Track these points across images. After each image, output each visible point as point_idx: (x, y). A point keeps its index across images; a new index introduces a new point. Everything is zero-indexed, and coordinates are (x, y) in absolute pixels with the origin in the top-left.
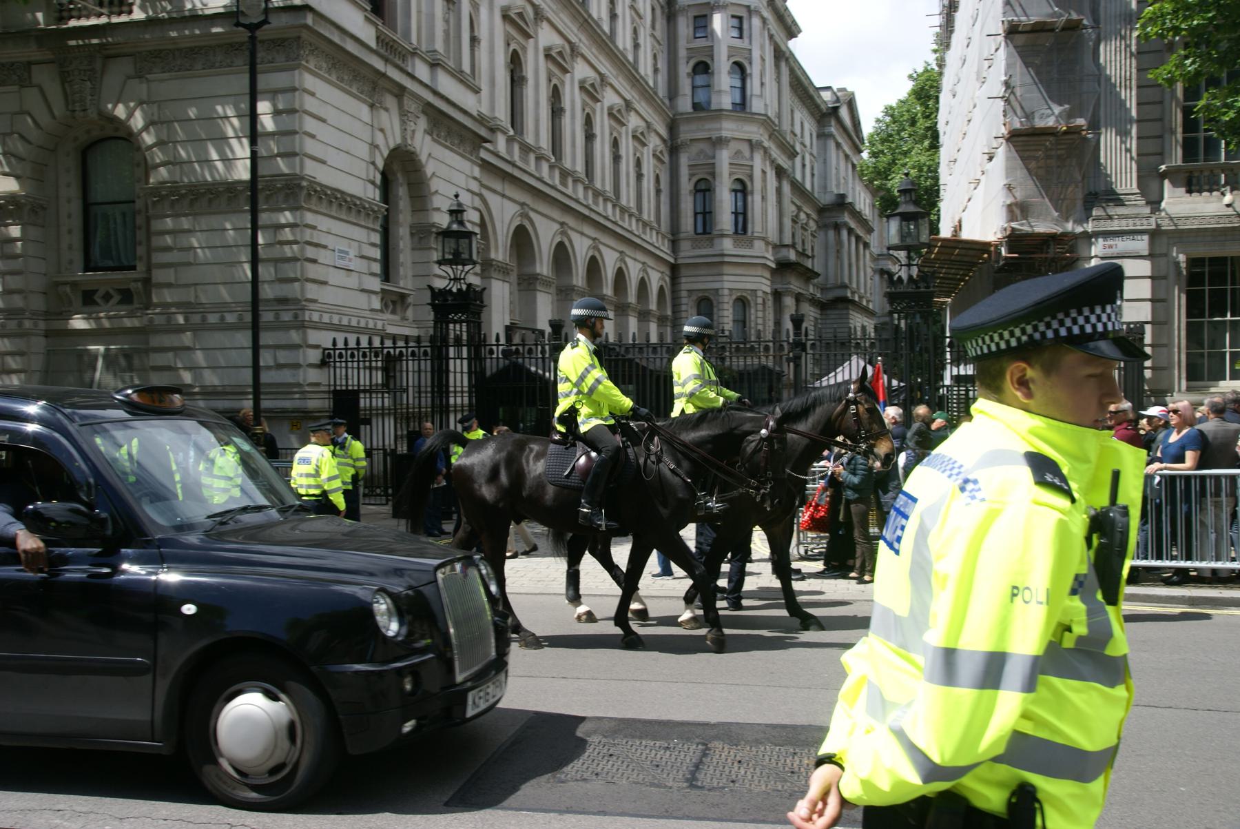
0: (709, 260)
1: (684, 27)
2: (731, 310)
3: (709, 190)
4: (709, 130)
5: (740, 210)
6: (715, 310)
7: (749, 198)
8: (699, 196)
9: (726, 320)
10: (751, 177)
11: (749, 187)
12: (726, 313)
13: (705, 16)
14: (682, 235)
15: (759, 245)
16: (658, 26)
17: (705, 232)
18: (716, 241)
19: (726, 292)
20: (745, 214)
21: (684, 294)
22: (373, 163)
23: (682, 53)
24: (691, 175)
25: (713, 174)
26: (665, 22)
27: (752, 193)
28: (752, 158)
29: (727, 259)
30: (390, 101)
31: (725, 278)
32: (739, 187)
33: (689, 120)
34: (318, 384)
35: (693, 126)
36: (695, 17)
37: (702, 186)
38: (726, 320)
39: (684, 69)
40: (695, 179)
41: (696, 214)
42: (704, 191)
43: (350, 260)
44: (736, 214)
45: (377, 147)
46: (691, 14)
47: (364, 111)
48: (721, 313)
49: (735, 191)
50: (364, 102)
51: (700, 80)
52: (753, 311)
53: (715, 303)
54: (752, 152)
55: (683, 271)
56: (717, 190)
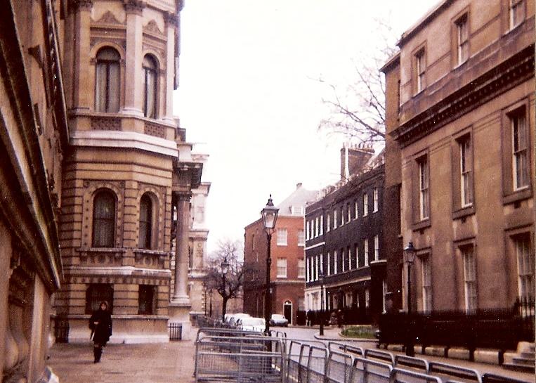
6: (120, 206)
7: (162, 79)
10: (164, 54)
11: (162, 67)
14: (79, 112)
19: (135, 185)
21: (79, 183)
24: (93, 41)
25: (124, 43)
27: (164, 73)
28: (166, 34)
31: (137, 168)
37: (108, 57)
40: (98, 46)
42: (108, 63)
53: (120, 198)
54: (166, 27)
55: (79, 156)
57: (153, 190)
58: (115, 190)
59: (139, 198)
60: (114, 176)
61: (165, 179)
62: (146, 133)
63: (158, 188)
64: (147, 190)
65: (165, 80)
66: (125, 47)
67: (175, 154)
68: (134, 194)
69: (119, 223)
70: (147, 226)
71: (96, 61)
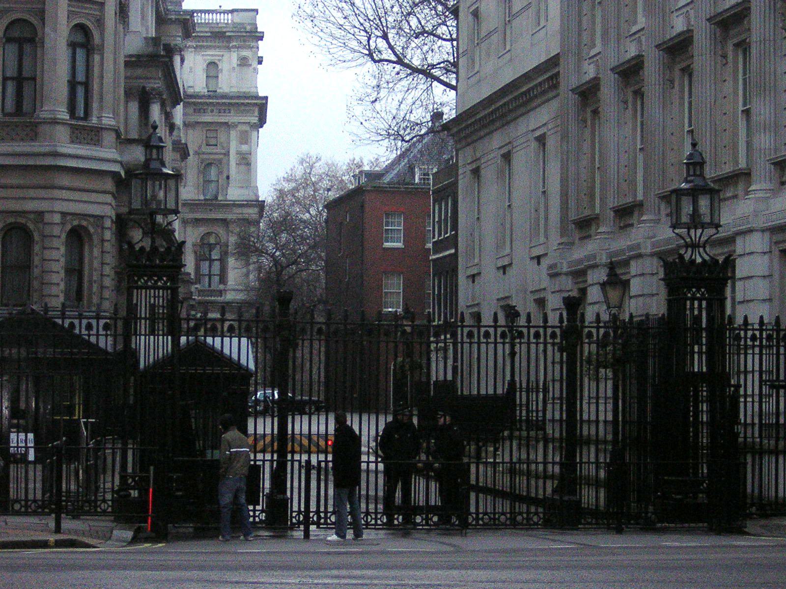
0: (22, 161)
2: (63, 249)
3: (32, 41)
5: (80, 77)
6: (37, 248)
7: (97, 58)
8: (12, 49)
9: (55, 267)
10: (100, 22)
12: (55, 255)
15: (109, 138)
17: (19, 109)
18: (44, 129)
19: (57, 218)
20: (87, 85)
25: (41, 14)
27: (101, 49)
29: (62, 162)
31: (57, 193)
32: (80, 38)
38: (55, 267)
41: (5, 79)
44: (73, 85)
48: (48, 254)
49: (73, 46)
52: (96, 252)
53: (37, 237)
56: (47, 40)
57: (84, 223)
58: (31, 226)
59: (64, 236)
60: (31, 206)
61: (102, 205)
62: (72, 142)
63: (92, 220)
64: (75, 223)
65: (102, 59)
66: (43, 21)
67: (116, 168)
68: (56, 231)
69: (36, 272)
70: (75, 271)
71: (4, 40)
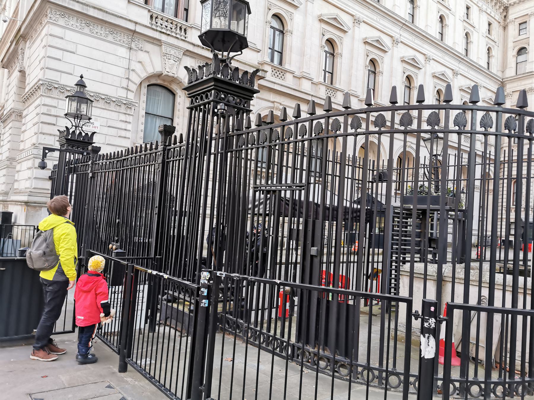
1: (513, 30)
4: (525, 85)
13: (526, 22)
16: (493, 32)
22: (128, 79)
23: (510, 45)
26: (501, 30)
30: (149, 47)
33: (513, 80)
34: (48, 190)
35: (515, 84)
36: (520, 24)
39: (512, 53)
43: (95, 127)
45: (133, 70)
46: (517, 24)
47: (123, 52)
50: (122, 46)
51: (521, 58)
